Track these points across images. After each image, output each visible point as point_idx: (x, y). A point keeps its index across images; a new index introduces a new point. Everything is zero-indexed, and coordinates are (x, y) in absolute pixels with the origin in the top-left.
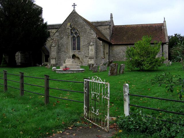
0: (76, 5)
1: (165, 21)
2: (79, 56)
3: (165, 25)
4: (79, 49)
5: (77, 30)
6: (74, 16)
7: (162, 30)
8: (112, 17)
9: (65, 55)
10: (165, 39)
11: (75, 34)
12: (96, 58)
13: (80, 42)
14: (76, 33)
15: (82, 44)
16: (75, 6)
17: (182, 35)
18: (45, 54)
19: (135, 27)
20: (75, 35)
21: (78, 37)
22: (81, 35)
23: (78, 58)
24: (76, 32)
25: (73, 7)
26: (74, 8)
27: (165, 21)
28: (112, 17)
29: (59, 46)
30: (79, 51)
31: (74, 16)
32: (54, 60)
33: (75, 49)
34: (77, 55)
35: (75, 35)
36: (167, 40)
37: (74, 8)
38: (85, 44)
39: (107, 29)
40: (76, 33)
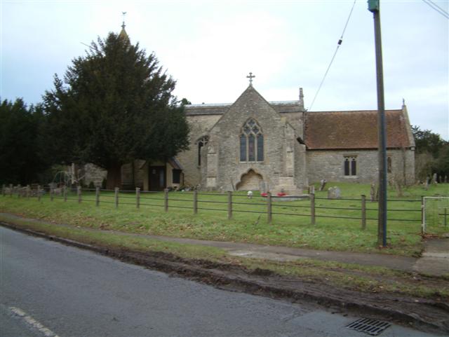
0: (254, 77)
1: (404, 106)
2: (262, 173)
3: (406, 113)
4: (261, 158)
5: (258, 124)
6: (250, 96)
7: (400, 122)
8: (301, 96)
9: (234, 170)
10: (408, 140)
11: (254, 130)
12: (296, 175)
13: (262, 147)
14: (255, 129)
15: (267, 148)
16: (253, 79)
17: (444, 137)
18: (172, 166)
19: (348, 116)
20: (253, 133)
21: (260, 137)
22: (265, 132)
23: (259, 176)
24: (255, 127)
25: (249, 79)
26: (251, 81)
27: (404, 106)
28: (301, 96)
29: (220, 153)
30: (262, 164)
31: (250, 96)
32: (214, 179)
33: (254, 160)
34: (258, 170)
35: (253, 133)
36: (412, 143)
37: (251, 81)
38: (272, 150)
39: (297, 119)
40: (255, 129)
